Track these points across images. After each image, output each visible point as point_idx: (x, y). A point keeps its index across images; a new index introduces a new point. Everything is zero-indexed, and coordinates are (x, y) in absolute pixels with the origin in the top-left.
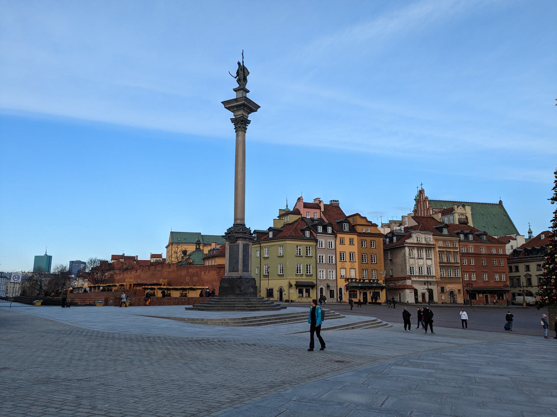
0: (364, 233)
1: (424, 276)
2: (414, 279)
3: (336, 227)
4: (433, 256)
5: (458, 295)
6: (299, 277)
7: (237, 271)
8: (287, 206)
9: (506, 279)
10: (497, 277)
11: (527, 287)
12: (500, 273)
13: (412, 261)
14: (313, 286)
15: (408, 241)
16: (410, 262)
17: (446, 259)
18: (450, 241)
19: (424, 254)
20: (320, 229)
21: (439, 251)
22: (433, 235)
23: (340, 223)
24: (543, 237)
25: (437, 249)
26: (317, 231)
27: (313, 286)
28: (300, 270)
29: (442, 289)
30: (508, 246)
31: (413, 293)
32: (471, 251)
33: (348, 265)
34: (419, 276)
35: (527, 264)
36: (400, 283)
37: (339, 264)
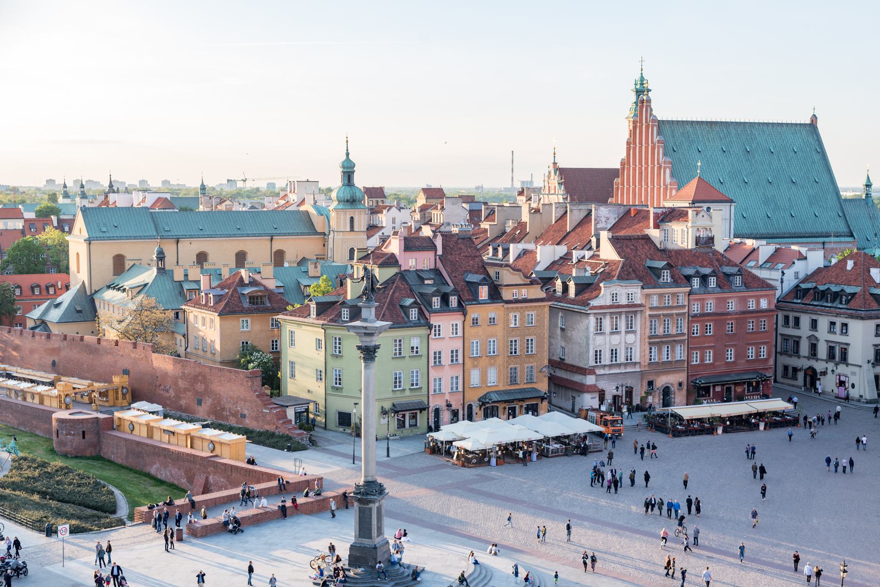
0: (517, 301)
1: (619, 365)
3: (466, 296)
4: (639, 326)
5: (677, 391)
6: (398, 395)
7: (370, 537)
8: (348, 154)
9: (769, 355)
10: (751, 353)
11: (808, 358)
12: (757, 345)
13: (599, 339)
14: (423, 409)
15: (594, 303)
17: (661, 330)
18: (674, 294)
19: (622, 326)
20: (436, 301)
21: (650, 316)
22: (643, 288)
23: (473, 288)
24: (850, 264)
25: (648, 313)
26: (431, 306)
27: (423, 409)
28: (400, 382)
29: (650, 383)
30: (790, 273)
31: (597, 399)
32: (711, 306)
33: (484, 361)
34: (611, 366)
35: (814, 317)
36: (577, 378)
37: (468, 363)
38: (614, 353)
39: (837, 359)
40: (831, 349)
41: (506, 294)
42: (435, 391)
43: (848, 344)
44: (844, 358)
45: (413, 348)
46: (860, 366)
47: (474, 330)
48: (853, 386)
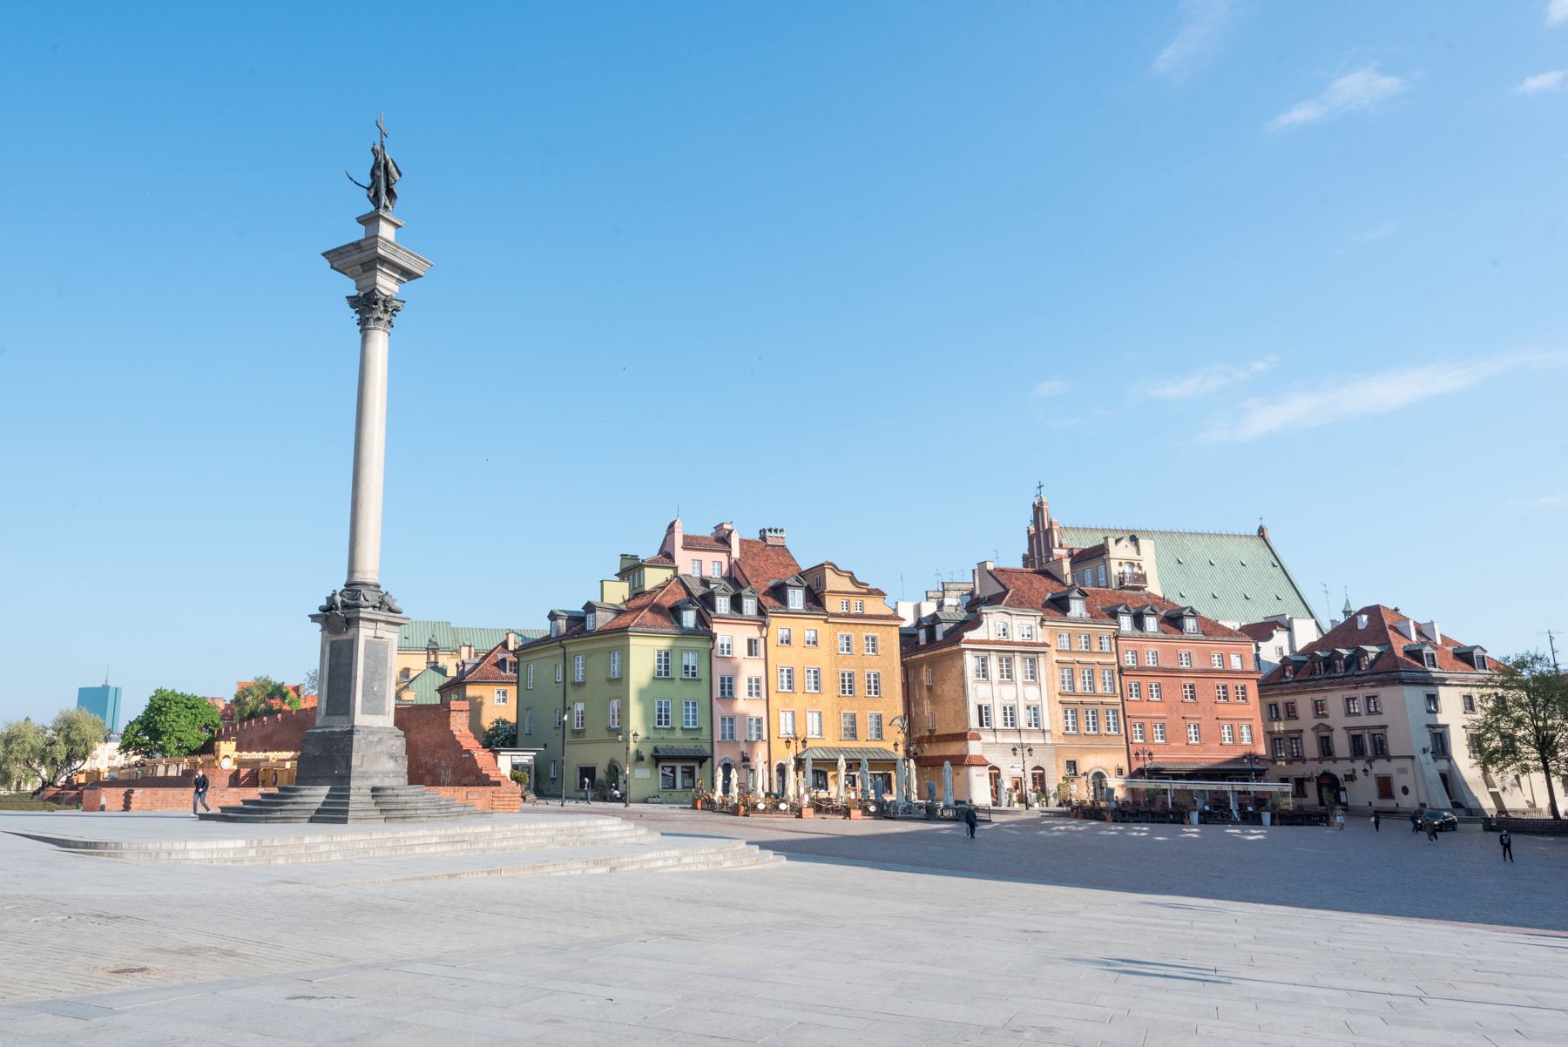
2: (988, 738)
11: (1320, 760)
15: (968, 635)
16: (978, 692)
20: (723, 605)
25: (1057, 657)
26: (714, 610)
29: (1072, 765)
38: (1010, 713)
39: (1369, 753)
40: (1356, 744)
41: (833, 604)
42: (724, 736)
43: (1384, 727)
44: (1381, 750)
45: (687, 667)
46: (1412, 758)
47: (785, 651)
48: (1405, 791)
